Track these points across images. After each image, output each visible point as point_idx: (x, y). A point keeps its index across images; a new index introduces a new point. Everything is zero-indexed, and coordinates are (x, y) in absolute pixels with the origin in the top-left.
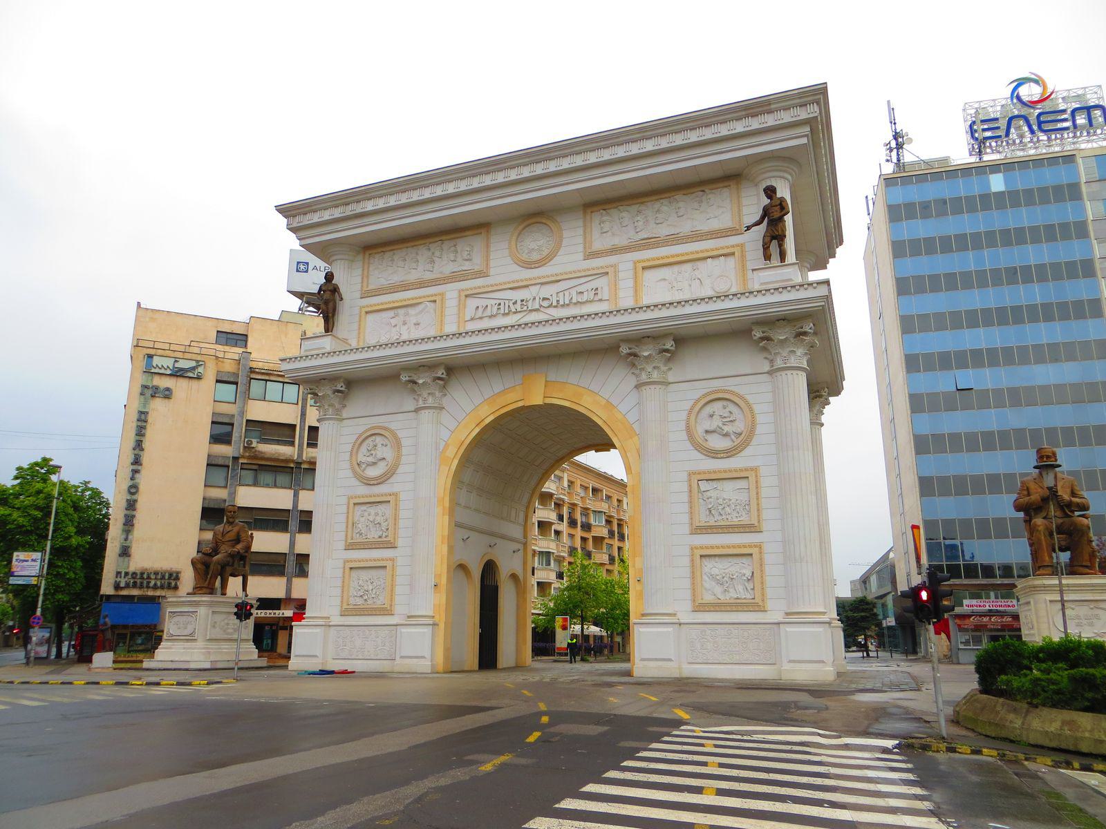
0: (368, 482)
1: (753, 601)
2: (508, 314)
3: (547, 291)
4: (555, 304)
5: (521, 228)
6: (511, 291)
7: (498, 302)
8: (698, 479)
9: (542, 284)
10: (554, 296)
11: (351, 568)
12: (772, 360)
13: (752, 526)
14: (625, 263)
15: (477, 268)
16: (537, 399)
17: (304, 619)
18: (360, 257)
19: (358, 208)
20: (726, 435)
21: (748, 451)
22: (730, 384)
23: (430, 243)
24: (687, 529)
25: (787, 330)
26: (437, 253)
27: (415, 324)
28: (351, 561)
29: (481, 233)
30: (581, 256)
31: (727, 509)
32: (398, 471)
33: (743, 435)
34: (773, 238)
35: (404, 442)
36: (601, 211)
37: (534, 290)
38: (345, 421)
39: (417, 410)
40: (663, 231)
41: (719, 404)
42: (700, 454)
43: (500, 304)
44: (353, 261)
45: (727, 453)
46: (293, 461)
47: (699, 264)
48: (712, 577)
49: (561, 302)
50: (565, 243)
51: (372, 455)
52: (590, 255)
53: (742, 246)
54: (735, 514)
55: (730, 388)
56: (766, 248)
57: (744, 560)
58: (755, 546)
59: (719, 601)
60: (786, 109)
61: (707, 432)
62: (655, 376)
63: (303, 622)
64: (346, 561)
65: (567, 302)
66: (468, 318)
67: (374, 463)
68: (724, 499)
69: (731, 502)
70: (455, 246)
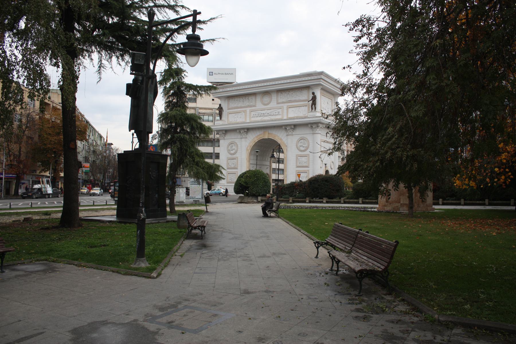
3: (269, 111)
8: (298, 156)
13: (307, 166)
14: (285, 106)
16: (266, 137)
18: (227, 99)
20: (304, 147)
22: (305, 136)
24: (295, 166)
30: (276, 103)
35: (239, 146)
37: (266, 111)
39: (241, 138)
40: (293, 99)
41: (303, 140)
46: (212, 139)
47: (300, 108)
50: (273, 100)
52: (278, 103)
56: (312, 106)
57: (306, 173)
60: (316, 75)
61: (300, 146)
62: (290, 133)
67: (232, 150)
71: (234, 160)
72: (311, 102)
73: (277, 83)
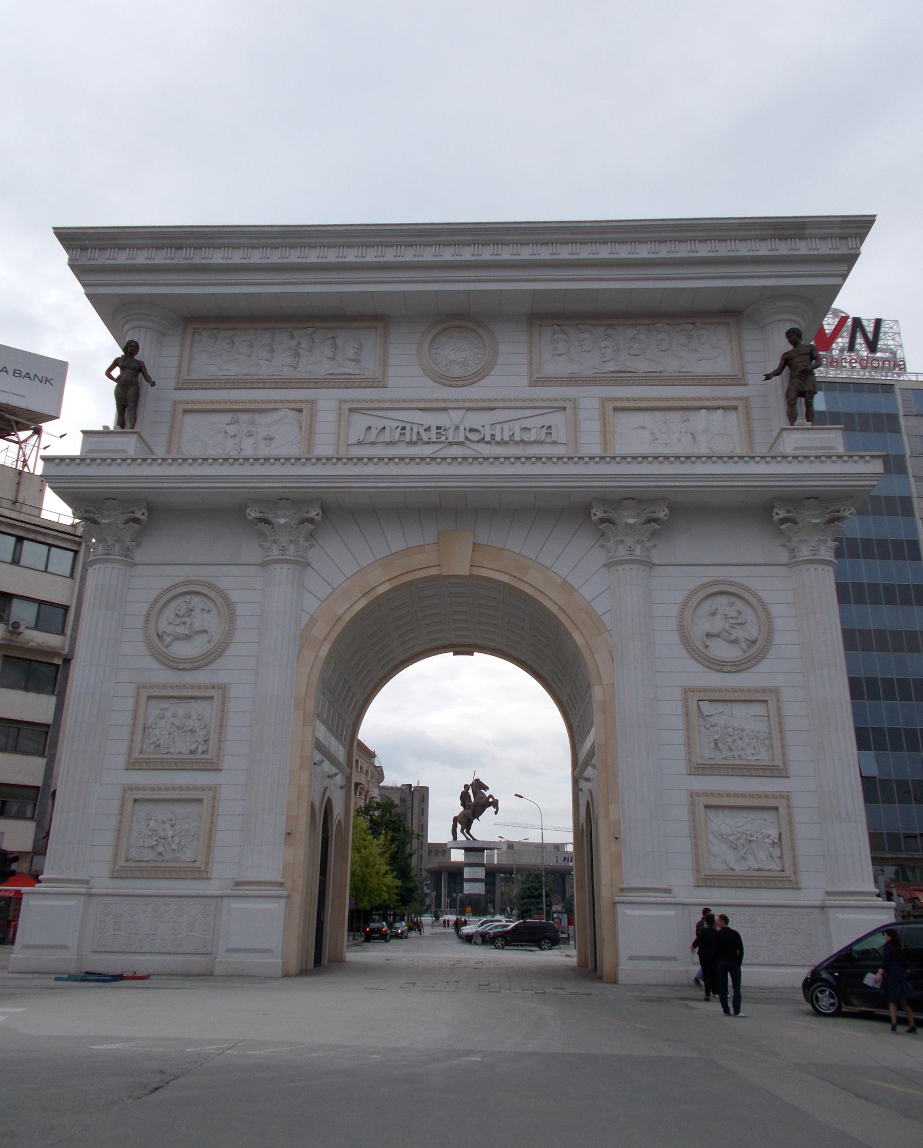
0: (174, 664)
1: (782, 874)
2: (415, 443)
4: (488, 438)
6: (420, 412)
7: (401, 425)
9: (468, 409)
10: (488, 428)
11: (135, 801)
12: (793, 550)
13: (774, 768)
15: (368, 374)
17: (40, 882)
20: (735, 642)
21: (764, 665)
23: (295, 329)
25: (817, 512)
26: (305, 344)
27: (265, 439)
28: (137, 789)
29: (376, 328)
30: (525, 381)
31: (739, 742)
32: (228, 653)
33: (759, 642)
34: (801, 394)
35: (240, 609)
36: (555, 326)
38: (138, 567)
40: (641, 366)
41: (724, 600)
42: (695, 663)
43: (404, 428)
45: (736, 666)
47: (691, 415)
48: (722, 837)
49: (498, 438)
51: (185, 623)
52: (538, 381)
53: (746, 399)
54: (750, 751)
55: (739, 580)
58: (782, 797)
59: (731, 873)
61: (708, 635)
63: (38, 887)
64: (127, 788)
65: (506, 438)
66: (353, 440)
67: (187, 637)
68: (734, 729)
69: (744, 734)
70: (333, 338)
71: (195, 708)
73: (564, 253)
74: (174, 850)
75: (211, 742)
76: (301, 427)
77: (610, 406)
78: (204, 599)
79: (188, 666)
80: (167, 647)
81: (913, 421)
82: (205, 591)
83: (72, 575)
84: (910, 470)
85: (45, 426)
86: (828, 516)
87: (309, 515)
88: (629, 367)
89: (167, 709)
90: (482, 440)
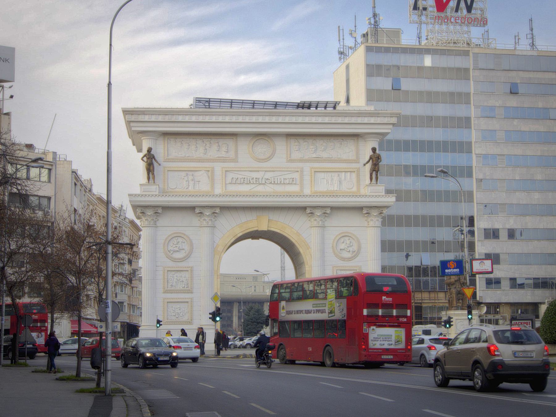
3: (269, 175)
4: (273, 183)
5: (255, 140)
6: (250, 172)
7: (244, 177)
10: (273, 178)
14: (307, 167)
19: (174, 118)
23: (204, 138)
33: (356, 252)
34: (374, 171)
40: (325, 155)
41: (347, 238)
43: (244, 178)
44: (157, 140)
49: (276, 182)
51: (177, 247)
65: (279, 183)
71: (183, 274)
72: (369, 166)
74: (181, 316)
75: (189, 284)
76: (209, 177)
77: (313, 170)
78: (182, 239)
79: (179, 261)
80: (171, 254)
81: (477, 73)
82: (182, 236)
83: (49, 181)
84: (472, 102)
85: (6, 85)
86: (379, 212)
87: (216, 211)
88: (321, 156)
89: (174, 274)
90: (271, 183)
